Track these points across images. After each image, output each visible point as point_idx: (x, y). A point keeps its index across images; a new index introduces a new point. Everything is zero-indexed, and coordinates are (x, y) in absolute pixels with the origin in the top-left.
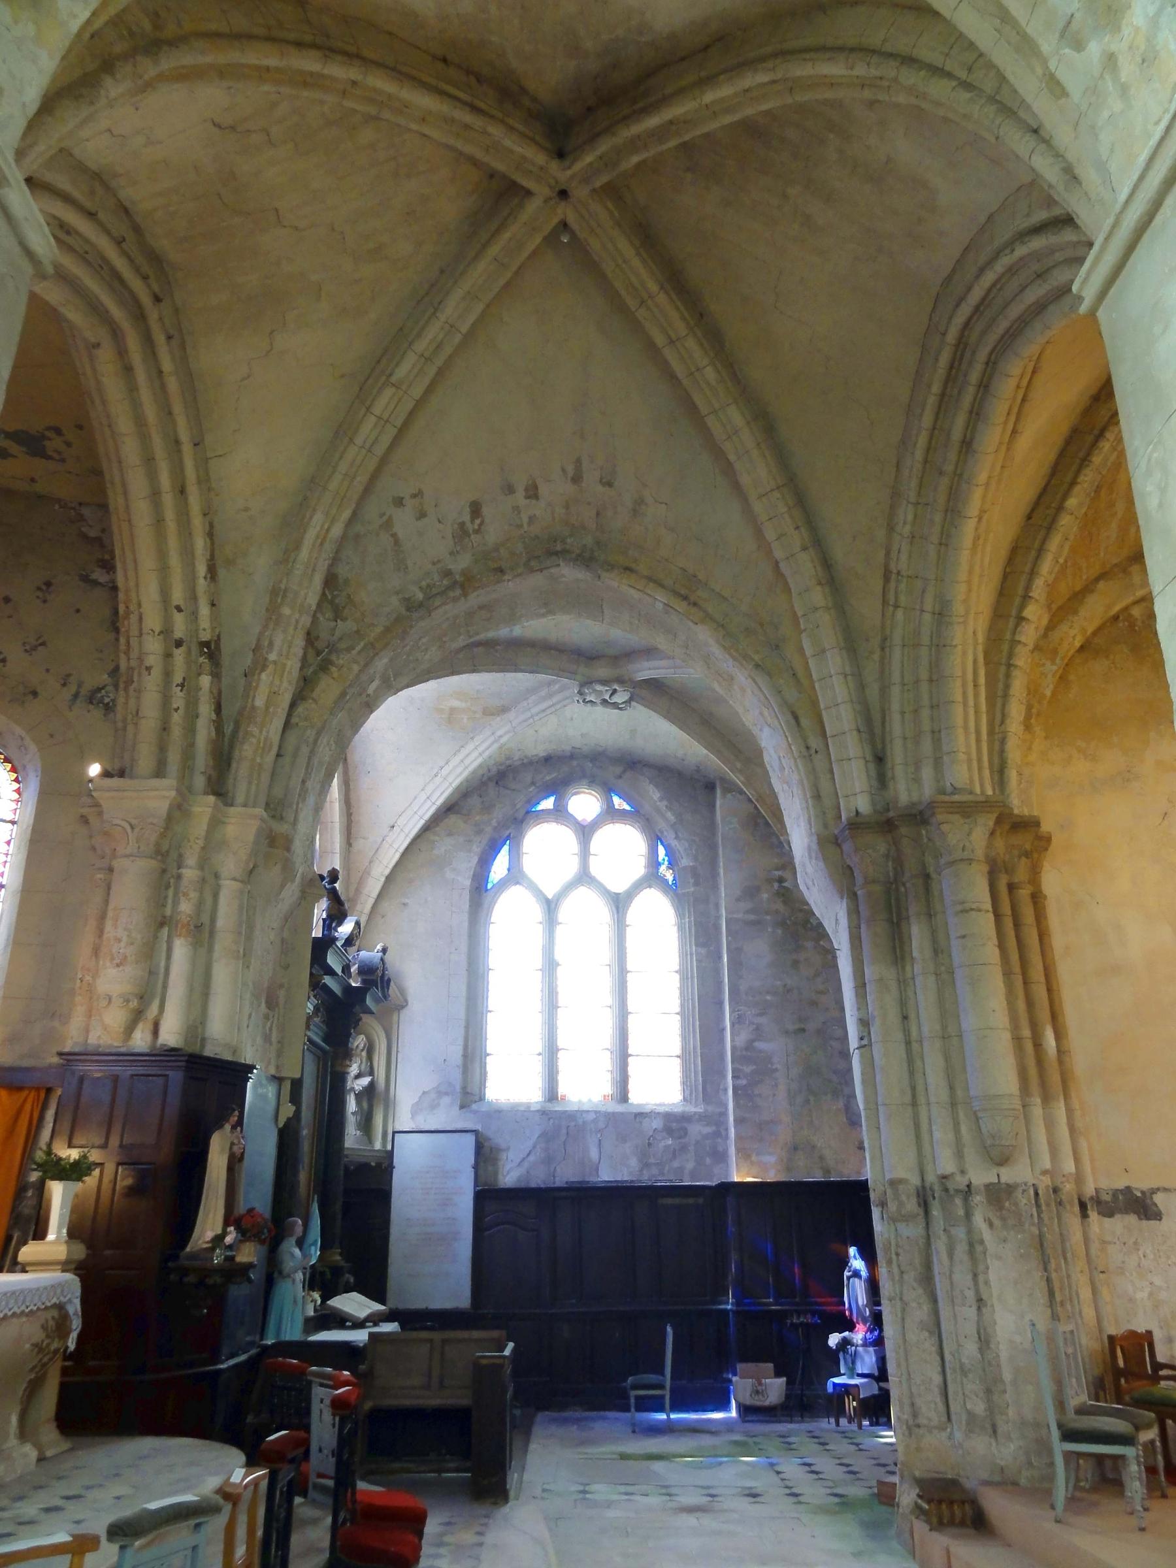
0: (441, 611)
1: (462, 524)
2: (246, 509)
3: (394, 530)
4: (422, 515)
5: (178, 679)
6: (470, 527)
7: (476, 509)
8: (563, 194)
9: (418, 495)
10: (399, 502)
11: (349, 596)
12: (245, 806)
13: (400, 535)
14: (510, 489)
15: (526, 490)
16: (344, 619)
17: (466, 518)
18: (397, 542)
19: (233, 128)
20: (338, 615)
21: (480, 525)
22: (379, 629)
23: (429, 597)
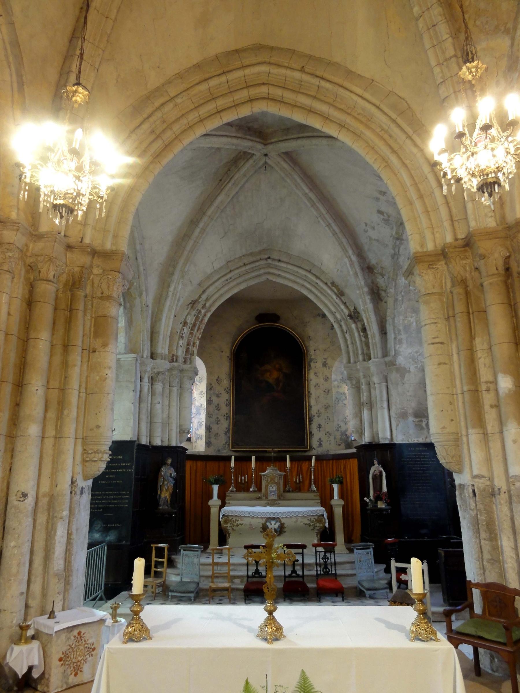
0: (401, 251)
1: (383, 219)
2: (338, 270)
3: (373, 238)
4: (374, 228)
5: (345, 331)
6: (386, 217)
7: (380, 212)
8: (266, 155)
9: (366, 224)
10: (366, 231)
11: (381, 267)
12: (375, 358)
13: (376, 238)
14: (378, 199)
15: (381, 194)
16: (385, 275)
17: (382, 217)
18: (378, 241)
19: (226, 233)
20: (383, 275)
21: (387, 214)
22: (392, 272)
23: (394, 250)
